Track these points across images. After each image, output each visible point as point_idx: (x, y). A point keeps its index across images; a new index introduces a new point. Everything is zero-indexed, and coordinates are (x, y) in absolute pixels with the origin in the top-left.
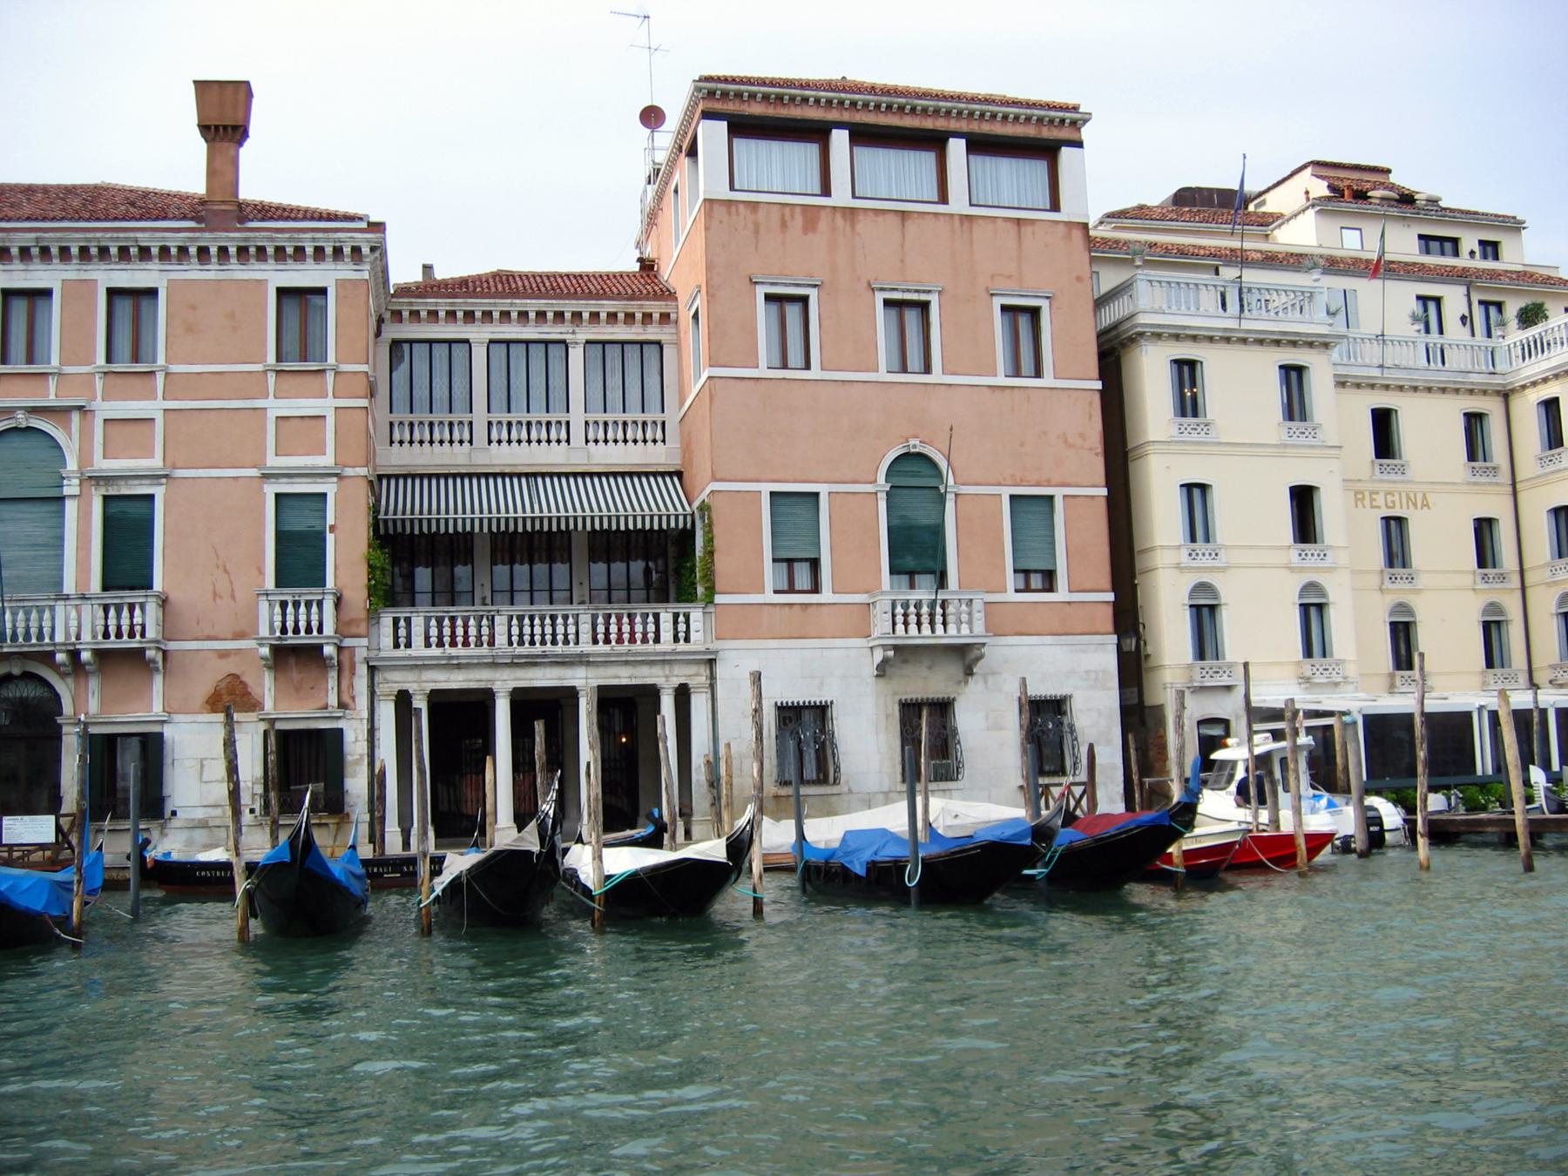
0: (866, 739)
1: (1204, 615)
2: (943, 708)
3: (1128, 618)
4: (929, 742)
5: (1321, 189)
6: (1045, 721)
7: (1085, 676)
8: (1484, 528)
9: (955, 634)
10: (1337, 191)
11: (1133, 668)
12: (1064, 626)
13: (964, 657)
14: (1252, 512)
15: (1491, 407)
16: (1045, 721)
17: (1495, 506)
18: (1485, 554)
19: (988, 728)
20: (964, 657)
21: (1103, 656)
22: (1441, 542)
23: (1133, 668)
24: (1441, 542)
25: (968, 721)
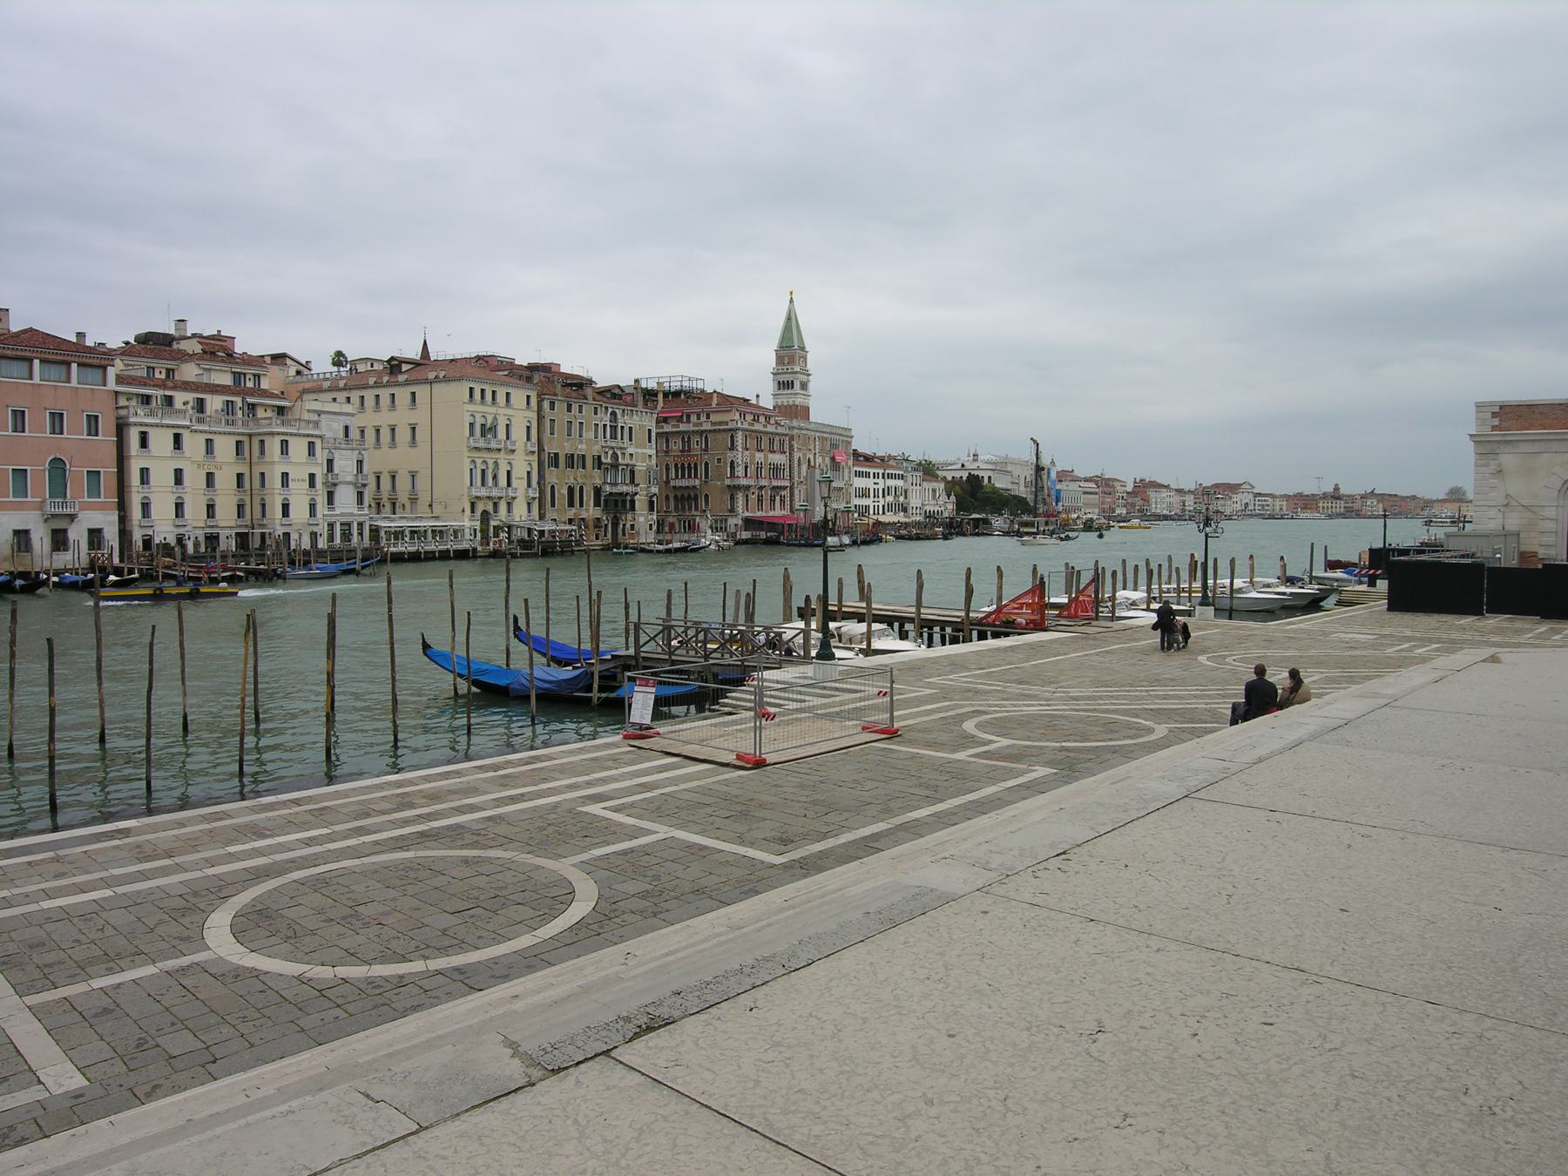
0: (41, 540)
1: (146, 506)
2: (65, 531)
3: (122, 507)
4: (59, 540)
5: (198, 349)
6: (95, 536)
7: (108, 523)
8: (240, 476)
9: (69, 511)
10: (204, 352)
11: (123, 520)
12: (102, 507)
13: (72, 517)
14: (162, 476)
15: (245, 439)
16: (95, 536)
17: (245, 470)
18: (240, 483)
19: (77, 534)
20: (72, 517)
21: (114, 517)
22: (226, 480)
23: (123, 520)
24: (226, 480)
25: (72, 535)
